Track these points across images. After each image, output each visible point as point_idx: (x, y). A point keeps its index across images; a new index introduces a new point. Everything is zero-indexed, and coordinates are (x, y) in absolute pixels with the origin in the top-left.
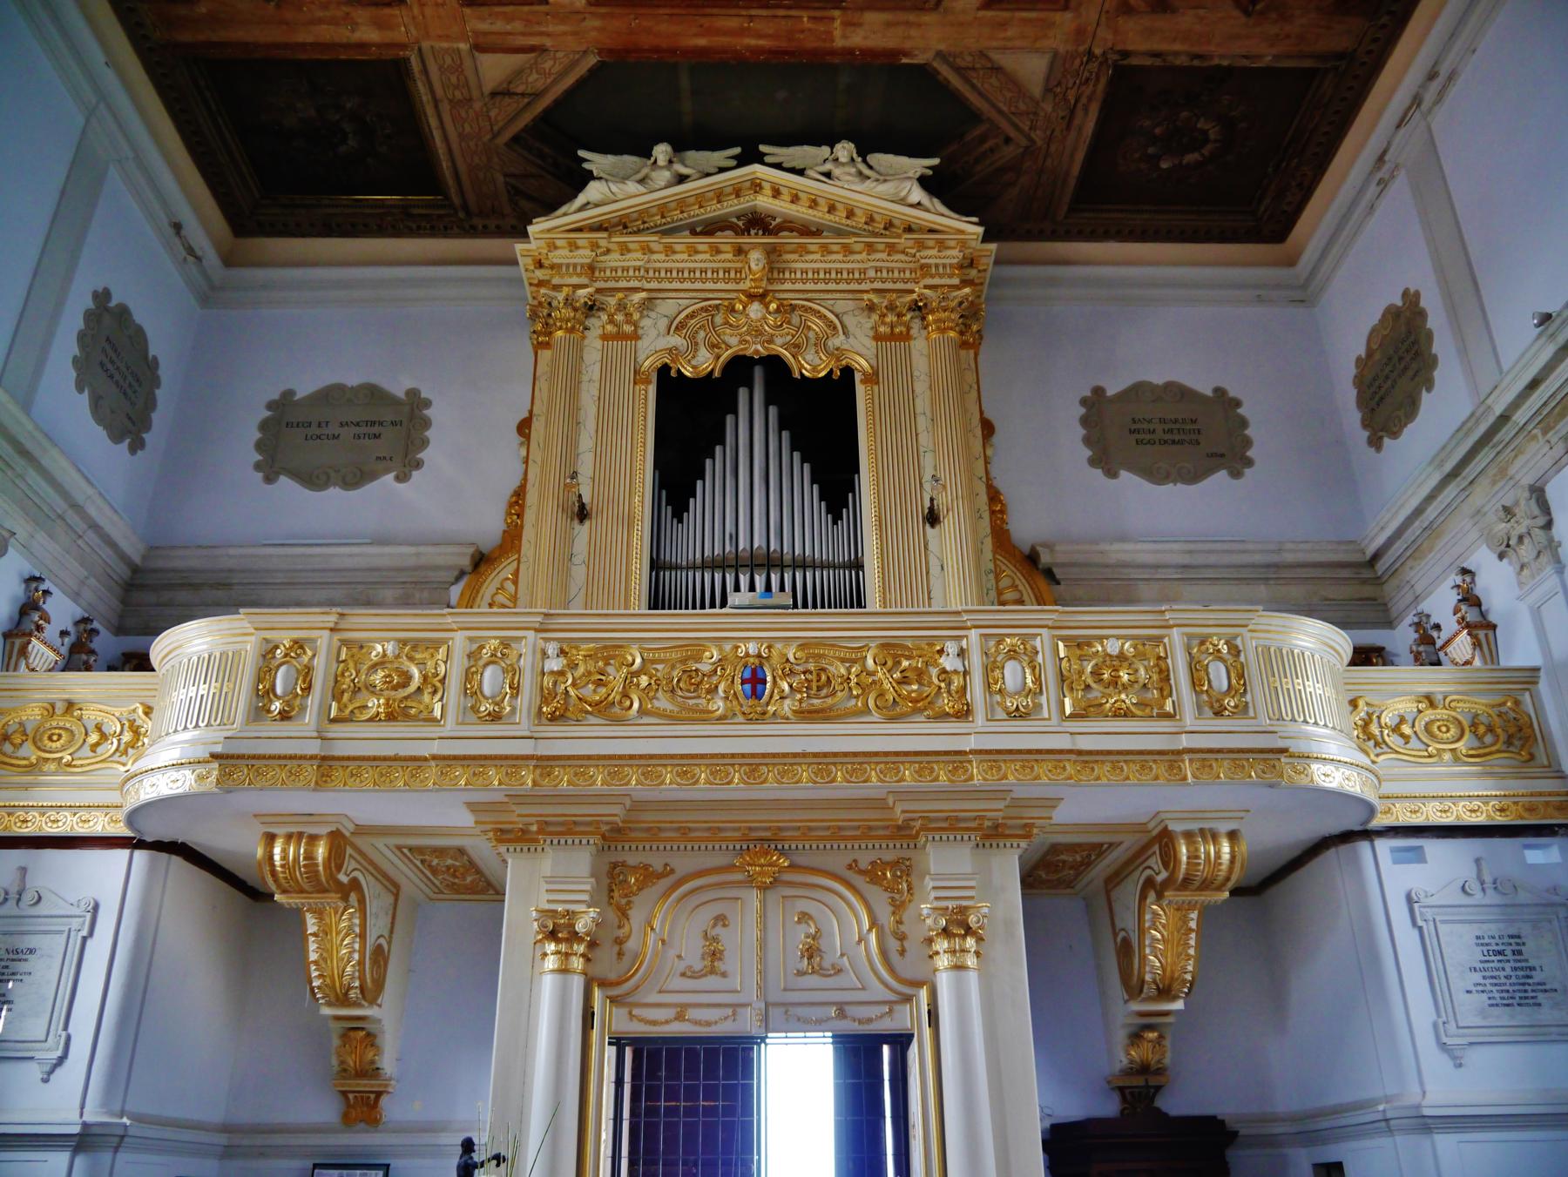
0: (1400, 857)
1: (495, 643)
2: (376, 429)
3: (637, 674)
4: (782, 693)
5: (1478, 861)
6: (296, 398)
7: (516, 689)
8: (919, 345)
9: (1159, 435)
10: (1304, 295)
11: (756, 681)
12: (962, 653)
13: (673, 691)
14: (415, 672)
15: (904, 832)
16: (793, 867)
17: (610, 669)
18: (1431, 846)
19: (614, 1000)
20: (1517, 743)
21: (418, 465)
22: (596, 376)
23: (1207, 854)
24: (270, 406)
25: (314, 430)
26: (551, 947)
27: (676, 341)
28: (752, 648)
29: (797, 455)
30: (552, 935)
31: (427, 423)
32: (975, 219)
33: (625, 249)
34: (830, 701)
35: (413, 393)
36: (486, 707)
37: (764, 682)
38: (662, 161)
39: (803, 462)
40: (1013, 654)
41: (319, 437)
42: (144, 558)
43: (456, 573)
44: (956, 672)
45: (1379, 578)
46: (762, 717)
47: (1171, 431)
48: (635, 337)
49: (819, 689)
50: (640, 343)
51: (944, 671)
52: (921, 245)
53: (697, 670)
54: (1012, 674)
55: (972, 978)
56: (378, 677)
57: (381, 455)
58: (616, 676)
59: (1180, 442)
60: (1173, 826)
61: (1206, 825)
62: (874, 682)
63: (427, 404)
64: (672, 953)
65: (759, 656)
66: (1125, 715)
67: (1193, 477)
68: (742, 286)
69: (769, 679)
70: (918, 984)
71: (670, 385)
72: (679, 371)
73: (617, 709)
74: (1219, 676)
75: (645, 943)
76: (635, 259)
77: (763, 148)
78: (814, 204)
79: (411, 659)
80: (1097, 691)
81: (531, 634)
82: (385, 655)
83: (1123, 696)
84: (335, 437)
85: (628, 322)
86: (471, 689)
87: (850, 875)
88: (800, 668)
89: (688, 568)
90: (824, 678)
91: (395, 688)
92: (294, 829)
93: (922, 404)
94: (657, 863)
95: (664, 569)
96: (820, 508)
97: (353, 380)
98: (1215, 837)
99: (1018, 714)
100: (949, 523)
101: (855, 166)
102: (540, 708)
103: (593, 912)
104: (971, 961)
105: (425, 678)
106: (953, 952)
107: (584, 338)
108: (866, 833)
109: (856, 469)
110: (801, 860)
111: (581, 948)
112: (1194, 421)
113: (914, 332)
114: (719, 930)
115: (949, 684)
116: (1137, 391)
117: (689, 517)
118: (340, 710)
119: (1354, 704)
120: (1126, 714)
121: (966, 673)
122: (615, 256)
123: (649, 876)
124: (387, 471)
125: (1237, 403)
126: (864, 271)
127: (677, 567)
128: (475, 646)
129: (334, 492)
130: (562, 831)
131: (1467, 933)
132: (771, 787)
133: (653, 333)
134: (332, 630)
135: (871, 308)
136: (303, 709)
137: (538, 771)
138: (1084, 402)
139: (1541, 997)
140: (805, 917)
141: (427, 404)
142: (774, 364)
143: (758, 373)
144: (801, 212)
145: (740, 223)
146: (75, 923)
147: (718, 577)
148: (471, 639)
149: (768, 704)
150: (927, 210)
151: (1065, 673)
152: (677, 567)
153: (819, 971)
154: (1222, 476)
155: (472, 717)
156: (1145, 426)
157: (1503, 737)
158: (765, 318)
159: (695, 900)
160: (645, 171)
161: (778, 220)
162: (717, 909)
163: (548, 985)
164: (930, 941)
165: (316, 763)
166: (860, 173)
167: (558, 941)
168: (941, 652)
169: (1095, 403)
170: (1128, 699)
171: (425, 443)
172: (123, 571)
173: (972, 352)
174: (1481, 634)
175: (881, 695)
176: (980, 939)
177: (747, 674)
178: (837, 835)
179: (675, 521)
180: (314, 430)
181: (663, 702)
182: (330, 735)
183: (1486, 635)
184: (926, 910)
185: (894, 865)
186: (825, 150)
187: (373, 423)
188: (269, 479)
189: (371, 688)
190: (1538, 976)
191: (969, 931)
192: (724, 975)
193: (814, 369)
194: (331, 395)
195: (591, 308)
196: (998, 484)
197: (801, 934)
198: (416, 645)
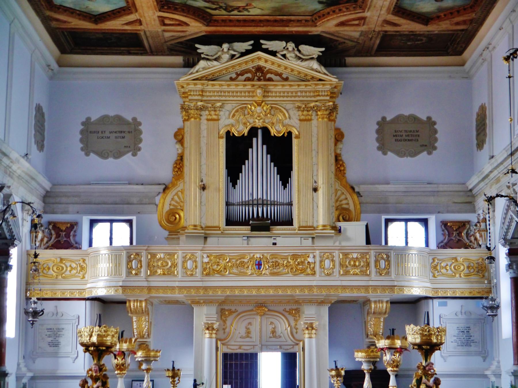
0: (440, 305)
1: (190, 255)
2: (123, 135)
3: (228, 262)
4: (265, 269)
5: (462, 306)
6: (92, 120)
7: (196, 267)
8: (314, 122)
9: (404, 137)
10: (468, 77)
11: (259, 265)
12: (314, 257)
13: (237, 267)
14: (170, 264)
15: (297, 302)
16: (269, 310)
17: (221, 261)
18: (449, 301)
19: (223, 344)
20: (480, 272)
21: (139, 149)
22: (205, 135)
23: (380, 306)
24: (83, 124)
25: (100, 135)
26: (207, 332)
27: (231, 121)
28: (258, 256)
29: (272, 164)
30: (208, 329)
31: (140, 132)
32: (335, 77)
33: (213, 85)
34: (279, 270)
35: (134, 119)
36: (189, 273)
37: (261, 265)
38: (226, 50)
39: (274, 166)
40: (328, 258)
41: (102, 138)
42: (51, 188)
43: (158, 193)
44: (312, 263)
45: (473, 195)
46: (260, 275)
47: (408, 135)
48: (218, 120)
49: (276, 266)
50: (219, 121)
51: (309, 262)
52: (316, 85)
53: (244, 261)
54: (327, 263)
55: (314, 340)
56: (160, 264)
57: (126, 145)
58: (222, 263)
59: (411, 140)
60: (371, 299)
61: (381, 299)
62: (290, 265)
63: (140, 124)
64: (237, 332)
65: (260, 258)
66: (356, 274)
67: (414, 154)
68: (254, 99)
69: (263, 264)
70: (300, 341)
71: (229, 137)
72: (233, 133)
73: (223, 272)
74: (383, 264)
75: (231, 330)
76: (217, 88)
77: (262, 41)
78: (279, 66)
79: (168, 259)
80: (349, 268)
81: (199, 252)
82: (161, 257)
83: (356, 270)
84: (108, 138)
85: (215, 115)
86: (184, 268)
87: (284, 313)
88: (271, 261)
89: (237, 205)
90: (277, 264)
91: (164, 266)
92: (135, 299)
93: (314, 146)
94: (233, 309)
95: (230, 205)
97: (112, 114)
98: (382, 302)
99: (328, 275)
100: (320, 192)
101: (294, 53)
102: (203, 272)
103: (218, 323)
104: (313, 336)
105: (172, 264)
106: (309, 334)
107: (200, 119)
108: (288, 302)
109: (291, 169)
110: (271, 308)
111: (214, 332)
112: (417, 131)
113: (313, 117)
114: (249, 326)
115: (310, 265)
116: (398, 119)
118: (151, 272)
119: (434, 260)
120: (357, 274)
121: (315, 263)
122: (210, 87)
123: (231, 312)
124: (128, 152)
125: (435, 123)
126: (296, 92)
127: (234, 205)
128: (185, 255)
129: (111, 160)
130: (208, 302)
131: (455, 326)
132: (263, 292)
133: (224, 118)
134: (146, 250)
135: (299, 107)
136: (141, 272)
137: (204, 290)
138: (378, 123)
139: (472, 344)
140: (272, 323)
141: (140, 124)
142: (266, 131)
143: (260, 132)
144: (275, 68)
145: (253, 70)
146: (74, 321)
147: (247, 208)
148: (183, 253)
149: (262, 271)
150: (320, 72)
151: (341, 262)
152: (234, 205)
153: (275, 337)
154: (425, 153)
155: (185, 275)
156: (399, 133)
157: (476, 270)
158: (261, 112)
159: (244, 318)
160: (219, 54)
161: (267, 69)
162: (249, 321)
163: (207, 341)
164: (304, 330)
165: (147, 288)
166: (296, 56)
167: (209, 330)
168: (308, 257)
169: (382, 124)
170: (357, 271)
171: (141, 141)
172: (43, 192)
173: (333, 123)
174: (483, 233)
175: (292, 269)
176: (316, 330)
177: (257, 263)
178: (280, 302)
179: (233, 188)
180: (100, 135)
181: (235, 270)
182: (149, 280)
183: (484, 233)
184: (302, 324)
185: (295, 310)
186: (284, 43)
187: (121, 132)
188: (87, 154)
189: (158, 267)
190: (472, 338)
191: (313, 328)
192: (251, 338)
193: (279, 132)
194: (104, 119)
195: (203, 109)
196: (345, 157)
197: (271, 327)
198: (169, 254)
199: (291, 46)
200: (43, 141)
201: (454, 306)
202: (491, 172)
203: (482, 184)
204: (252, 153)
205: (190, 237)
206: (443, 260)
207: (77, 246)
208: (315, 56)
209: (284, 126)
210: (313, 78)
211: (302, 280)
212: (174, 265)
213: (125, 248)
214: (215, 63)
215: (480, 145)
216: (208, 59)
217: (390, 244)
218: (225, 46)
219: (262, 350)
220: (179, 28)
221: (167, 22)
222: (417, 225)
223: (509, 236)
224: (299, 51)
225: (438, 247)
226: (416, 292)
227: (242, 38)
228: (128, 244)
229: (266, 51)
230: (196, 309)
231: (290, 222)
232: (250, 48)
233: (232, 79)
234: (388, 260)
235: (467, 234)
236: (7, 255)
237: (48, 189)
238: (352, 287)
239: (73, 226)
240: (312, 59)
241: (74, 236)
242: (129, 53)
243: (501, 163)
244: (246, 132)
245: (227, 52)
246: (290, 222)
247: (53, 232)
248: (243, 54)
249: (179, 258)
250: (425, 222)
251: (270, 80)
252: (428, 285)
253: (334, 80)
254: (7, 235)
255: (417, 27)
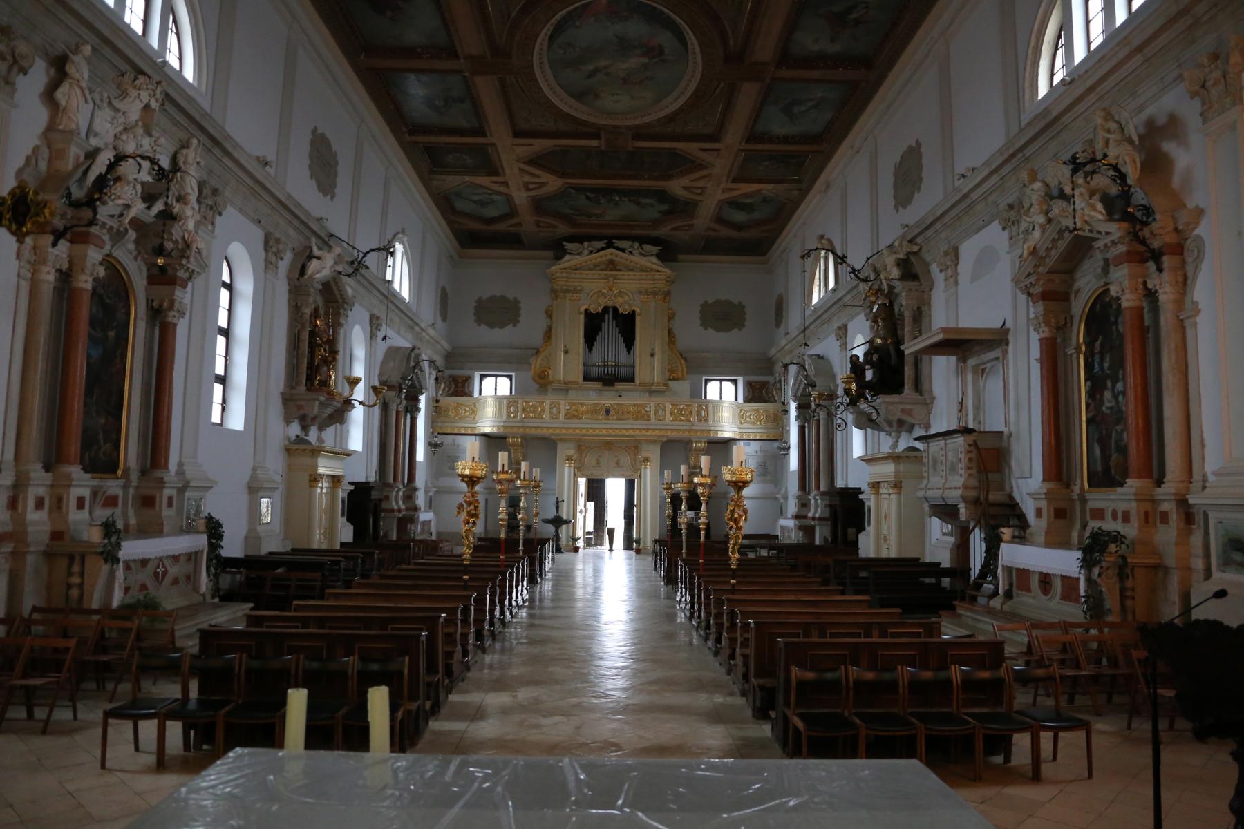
11: (608, 412)
18: (752, 442)
30: (568, 460)
31: (519, 309)
35: (515, 299)
46: (609, 419)
48: (579, 300)
55: (648, 471)
67: (728, 330)
77: (614, 241)
96: (625, 350)
100: (656, 357)
109: (633, 339)
116: (717, 302)
117: (592, 352)
124: (509, 324)
125: (744, 307)
129: (496, 330)
138: (702, 306)
142: (615, 309)
143: (611, 310)
154: (736, 330)
171: (519, 315)
194: (493, 299)
199: (636, 245)
200: (446, 314)
201: (755, 446)
202: (786, 345)
203: (778, 355)
204: (605, 326)
205: (556, 390)
206: (747, 411)
207: (470, 394)
208: (654, 253)
209: (629, 306)
210: (652, 270)
211: (640, 424)
212: (543, 410)
213: (505, 397)
214: (577, 257)
215: (778, 324)
216: (571, 254)
217: (708, 398)
218: (586, 244)
219: (608, 477)
220: (550, 229)
221: (542, 224)
222: (729, 383)
223: (799, 394)
224: (642, 249)
225: (745, 401)
226: (727, 434)
227: (599, 238)
228: (508, 394)
229: (617, 248)
230: (559, 446)
231: (631, 379)
232: (605, 245)
233: (590, 269)
234: (707, 410)
235: (766, 392)
236: (418, 400)
237: (449, 351)
238: (678, 431)
239: (468, 380)
240: (652, 255)
241: (468, 387)
242: (512, 249)
243: (794, 339)
244: (600, 309)
245: (587, 249)
246: (631, 379)
247: (453, 384)
248: (599, 250)
249: (547, 404)
250: (735, 382)
251: (619, 270)
252: (736, 430)
253: (668, 271)
254: (417, 384)
255: (734, 234)
